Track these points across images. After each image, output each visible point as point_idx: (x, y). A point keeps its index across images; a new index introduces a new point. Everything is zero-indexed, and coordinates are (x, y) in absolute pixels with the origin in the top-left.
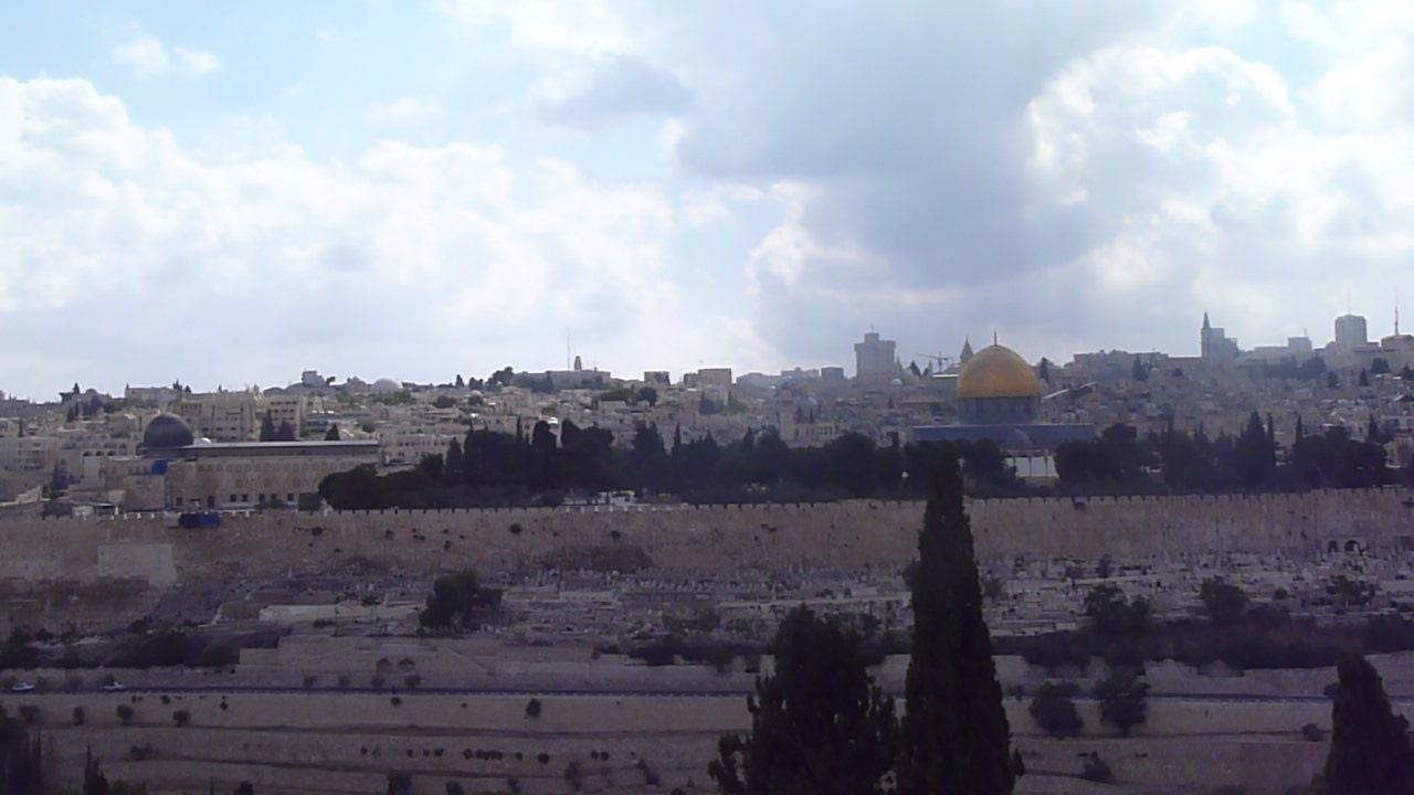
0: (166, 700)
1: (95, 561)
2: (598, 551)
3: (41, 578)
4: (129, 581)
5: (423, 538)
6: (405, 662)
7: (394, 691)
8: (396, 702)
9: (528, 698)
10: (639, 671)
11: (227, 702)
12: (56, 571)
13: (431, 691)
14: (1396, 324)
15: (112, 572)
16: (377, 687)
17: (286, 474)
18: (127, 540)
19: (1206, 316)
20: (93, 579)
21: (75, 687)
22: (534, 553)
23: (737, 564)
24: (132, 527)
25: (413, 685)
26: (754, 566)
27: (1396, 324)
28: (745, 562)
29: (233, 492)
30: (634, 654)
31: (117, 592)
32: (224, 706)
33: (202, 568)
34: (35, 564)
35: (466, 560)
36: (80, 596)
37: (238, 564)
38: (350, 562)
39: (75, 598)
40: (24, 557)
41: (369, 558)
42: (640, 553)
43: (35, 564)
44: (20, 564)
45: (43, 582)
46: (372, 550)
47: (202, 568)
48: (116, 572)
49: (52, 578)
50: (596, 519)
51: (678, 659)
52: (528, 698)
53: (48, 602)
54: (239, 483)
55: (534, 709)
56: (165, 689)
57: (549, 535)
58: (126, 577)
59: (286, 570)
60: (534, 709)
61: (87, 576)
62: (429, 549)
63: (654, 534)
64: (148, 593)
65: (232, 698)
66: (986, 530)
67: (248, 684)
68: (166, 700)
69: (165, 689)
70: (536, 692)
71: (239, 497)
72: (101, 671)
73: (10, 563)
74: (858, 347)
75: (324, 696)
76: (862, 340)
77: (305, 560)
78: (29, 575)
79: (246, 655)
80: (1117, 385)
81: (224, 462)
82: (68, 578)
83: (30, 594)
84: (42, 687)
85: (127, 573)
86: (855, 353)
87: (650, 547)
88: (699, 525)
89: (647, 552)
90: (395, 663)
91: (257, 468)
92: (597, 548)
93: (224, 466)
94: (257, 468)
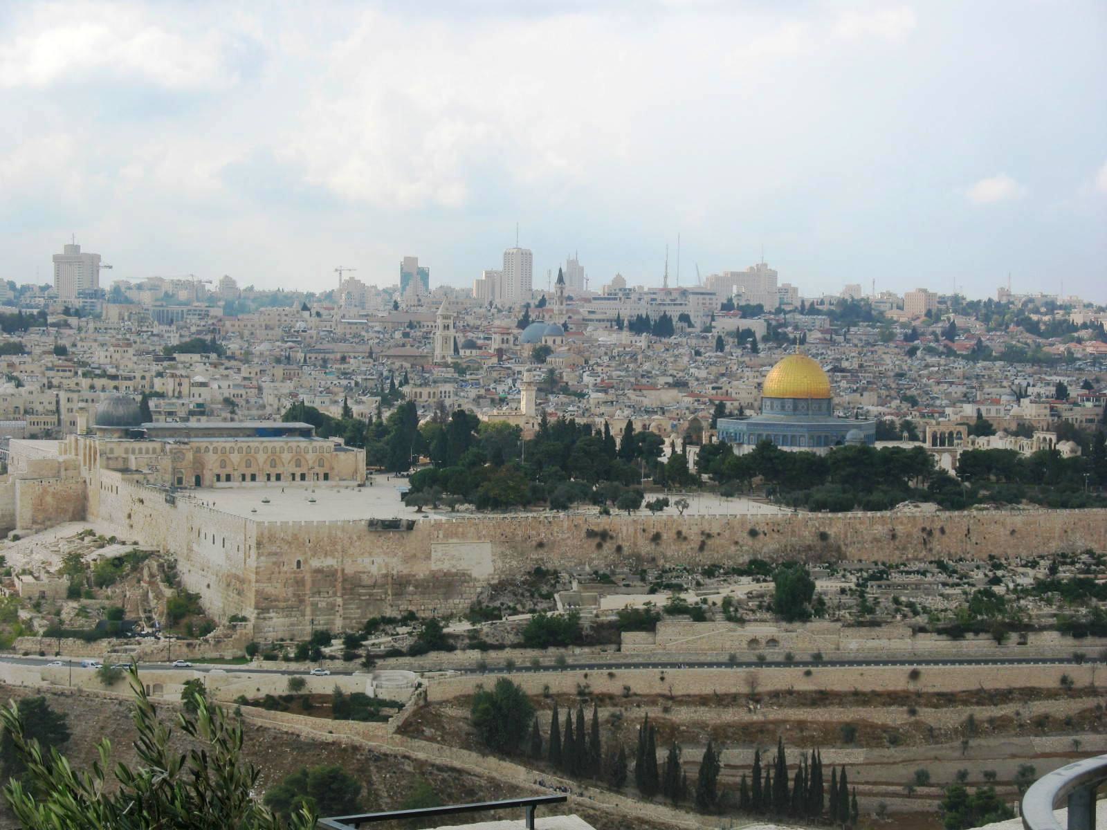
0: (611, 675)
1: (428, 557)
2: (809, 548)
3: (384, 572)
4: (456, 574)
5: (685, 539)
6: (773, 642)
7: (805, 664)
8: (808, 673)
9: (908, 668)
10: (942, 645)
11: (665, 675)
12: (397, 567)
13: (833, 663)
14: (666, 277)
15: (441, 567)
16: (789, 661)
17: (265, 456)
18: (455, 540)
19: (560, 270)
20: (427, 573)
21: (536, 667)
22: (765, 550)
23: (905, 557)
24: (461, 529)
25: (818, 660)
26: (916, 559)
27: (666, 277)
28: (910, 556)
29: (217, 471)
30: (940, 632)
31: (447, 583)
32: (662, 679)
33: (514, 563)
34: (379, 560)
35: (716, 555)
36: (416, 587)
37: (542, 559)
38: (629, 557)
39: (411, 588)
40: (370, 554)
41: (643, 553)
42: (839, 547)
43: (379, 560)
44: (367, 560)
45: (386, 576)
46: (646, 548)
47: (514, 563)
48: (446, 566)
49: (395, 572)
50: (810, 523)
51: (970, 635)
52: (908, 668)
53: (390, 592)
54: (223, 464)
55: (915, 675)
56: (609, 666)
57: (776, 536)
58: (454, 570)
59: (581, 563)
60: (915, 675)
61: (421, 570)
62: (689, 547)
63: (849, 535)
64: (471, 584)
65: (669, 671)
66: (1066, 532)
67: (641, 660)
68: (611, 675)
69: (609, 666)
70: (919, 663)
71: (223, 477)
72: (507, 654)
73: (360, 560)
74: (57, 259)
75: (773, 669)
76: (61, 251)
77: (593, 556)
78: (374, 570)
79: (626, 636)
80: (554, 341)
81: (211, 443)
82: (405, 572)
83: (374, 586)
84: (510, 666)
85: (454, 566)
86: (52, 264)
87: (846, 545)
88: (880, 528)
89: (843, 548)
90: (763, 642)
91: (240, 450)
92: (809, 546)
93: (211, 448)
94: (240, 450)
